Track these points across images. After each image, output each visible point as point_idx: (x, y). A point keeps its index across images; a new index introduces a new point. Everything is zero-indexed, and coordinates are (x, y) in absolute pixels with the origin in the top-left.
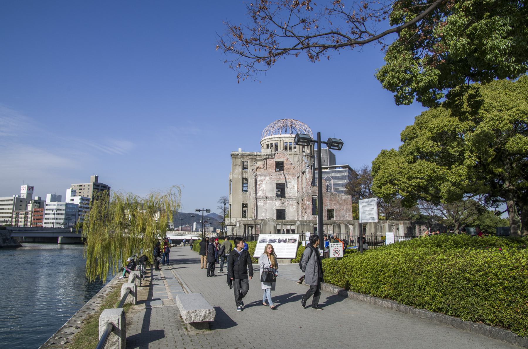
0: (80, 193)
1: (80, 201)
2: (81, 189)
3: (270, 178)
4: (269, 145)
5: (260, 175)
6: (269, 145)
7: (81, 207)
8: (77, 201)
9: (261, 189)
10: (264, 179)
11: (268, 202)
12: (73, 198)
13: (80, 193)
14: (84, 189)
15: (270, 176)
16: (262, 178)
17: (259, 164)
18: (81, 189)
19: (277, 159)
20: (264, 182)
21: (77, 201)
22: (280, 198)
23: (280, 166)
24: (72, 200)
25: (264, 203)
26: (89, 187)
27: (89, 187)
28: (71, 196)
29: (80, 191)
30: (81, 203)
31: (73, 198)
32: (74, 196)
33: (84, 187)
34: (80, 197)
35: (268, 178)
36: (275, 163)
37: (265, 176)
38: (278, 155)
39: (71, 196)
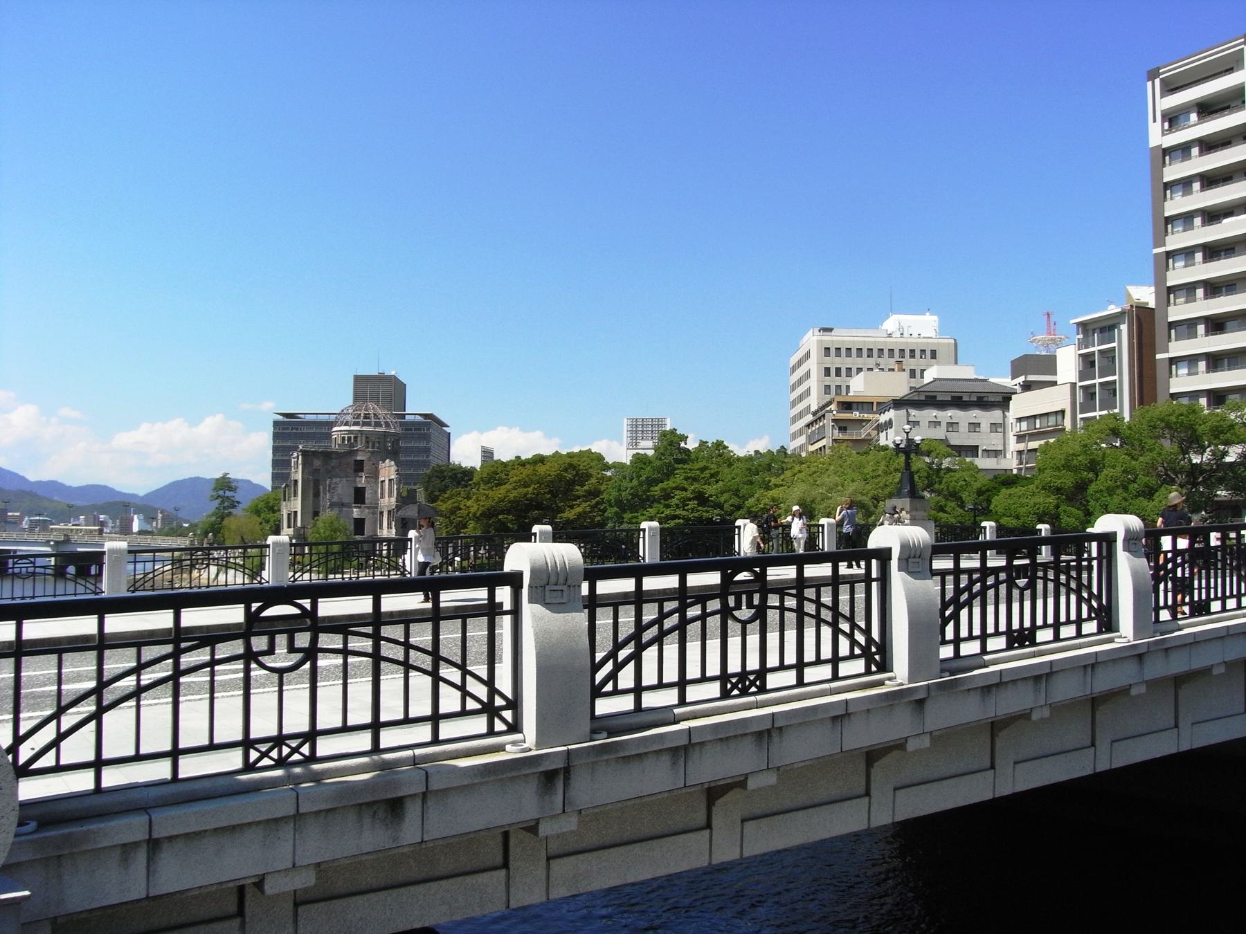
3: (347, 480)
4: (346, 438)
5: (336, 477)
6: (346, 438)
9: (336, 493)
11: (344, 509)
15: (347, 477)
16: (338, 480)
17: (334, 463)
19: (359, 458)
20: (340, 485)
22: (359, 505)
23: (359, 466)
25: (340, 511)
35: (345, 479)
36: (353, 462)
38: (359, 453)
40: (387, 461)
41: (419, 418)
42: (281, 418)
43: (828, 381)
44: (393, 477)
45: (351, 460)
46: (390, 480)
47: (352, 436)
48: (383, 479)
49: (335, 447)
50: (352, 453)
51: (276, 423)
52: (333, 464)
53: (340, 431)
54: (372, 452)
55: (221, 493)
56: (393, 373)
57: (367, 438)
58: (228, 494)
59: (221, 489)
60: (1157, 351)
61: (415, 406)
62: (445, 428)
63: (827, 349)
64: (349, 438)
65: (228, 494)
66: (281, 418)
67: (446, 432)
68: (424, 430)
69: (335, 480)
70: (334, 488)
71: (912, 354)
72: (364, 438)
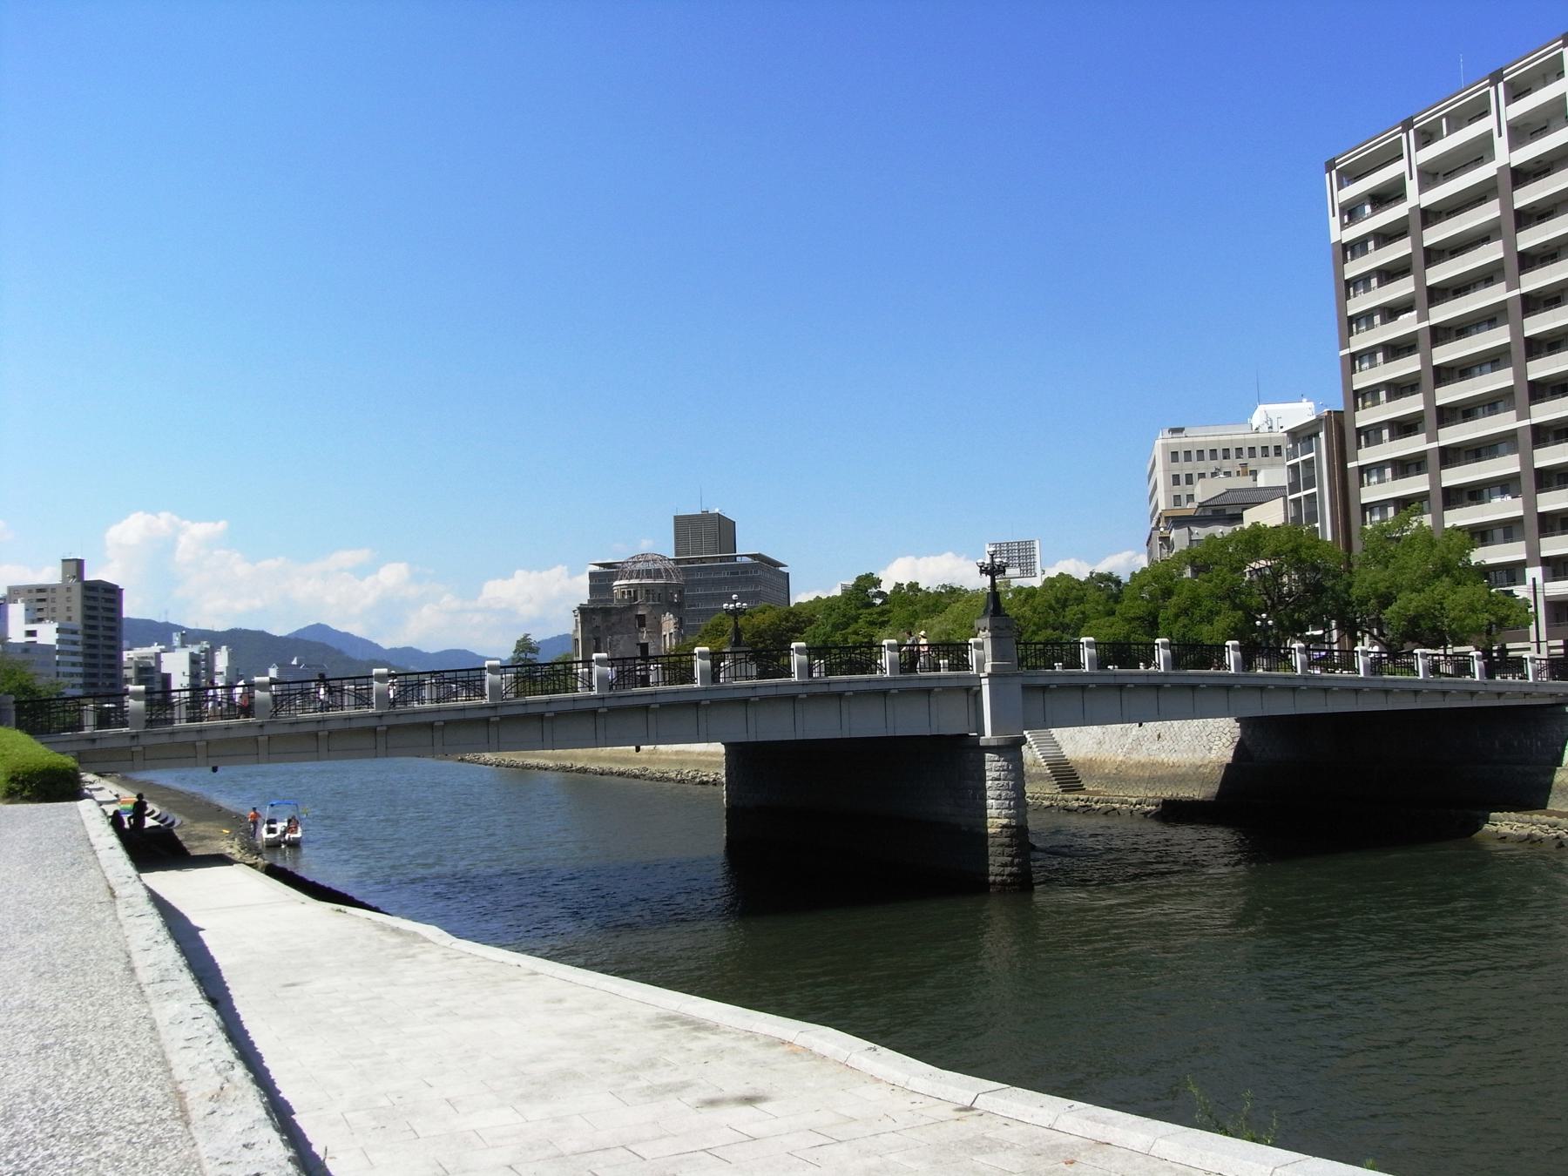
0: (40, 610)
1: (56, 636)
2: (44, 600)
5: (616, 633)
7: (58, 652)
8: (47, 634)
10: (622, 638)
12: (31, 627)
13: (40, 610)
14: (53, 601)
16: (620, 636)
17: (614, 619)
18: (44, 600)
19: (639, 613)
20: (622, 642)
21: (47, 634)
23: (641, 620)
24: (32, 633)
26: (68, 594)
27: (68, 594)
28: (26, 623)
29: (41, 605)
30: (58, 641)
31: (31, 627)
32: (33, 622)
33: (52, 595)
34: (56, 625)
37: (623, 634)
39: (26, 623)
40: (668, 613)
41: (749, 560)
42: (597, 568)
43: (1177, 490)
44: (672, 631)
45: (631, 615)
46: (671, 634)
47: (632, 590)
48: (664, 633)
49: (615, 604)
50: (631, 608)
51: (592, 575)
52: (613, 621)
53: (620, 585)
54: (653, 606)
55: (523, 655)
56: (717, 510)
57: (647, 591)
58: (530, 656)
59: (523, 651)
60: (1348, 460)
61: (747, 545)
62: (781, 569)
63: (1175, 455)
64: (629, 592)
65: (530, 656)
66: (597, 568)
67: (784, 573)
68: (751, 573)
69: (616, 637)
70: (615, 646)
71: (1279, 452)
72: (644, 592)
